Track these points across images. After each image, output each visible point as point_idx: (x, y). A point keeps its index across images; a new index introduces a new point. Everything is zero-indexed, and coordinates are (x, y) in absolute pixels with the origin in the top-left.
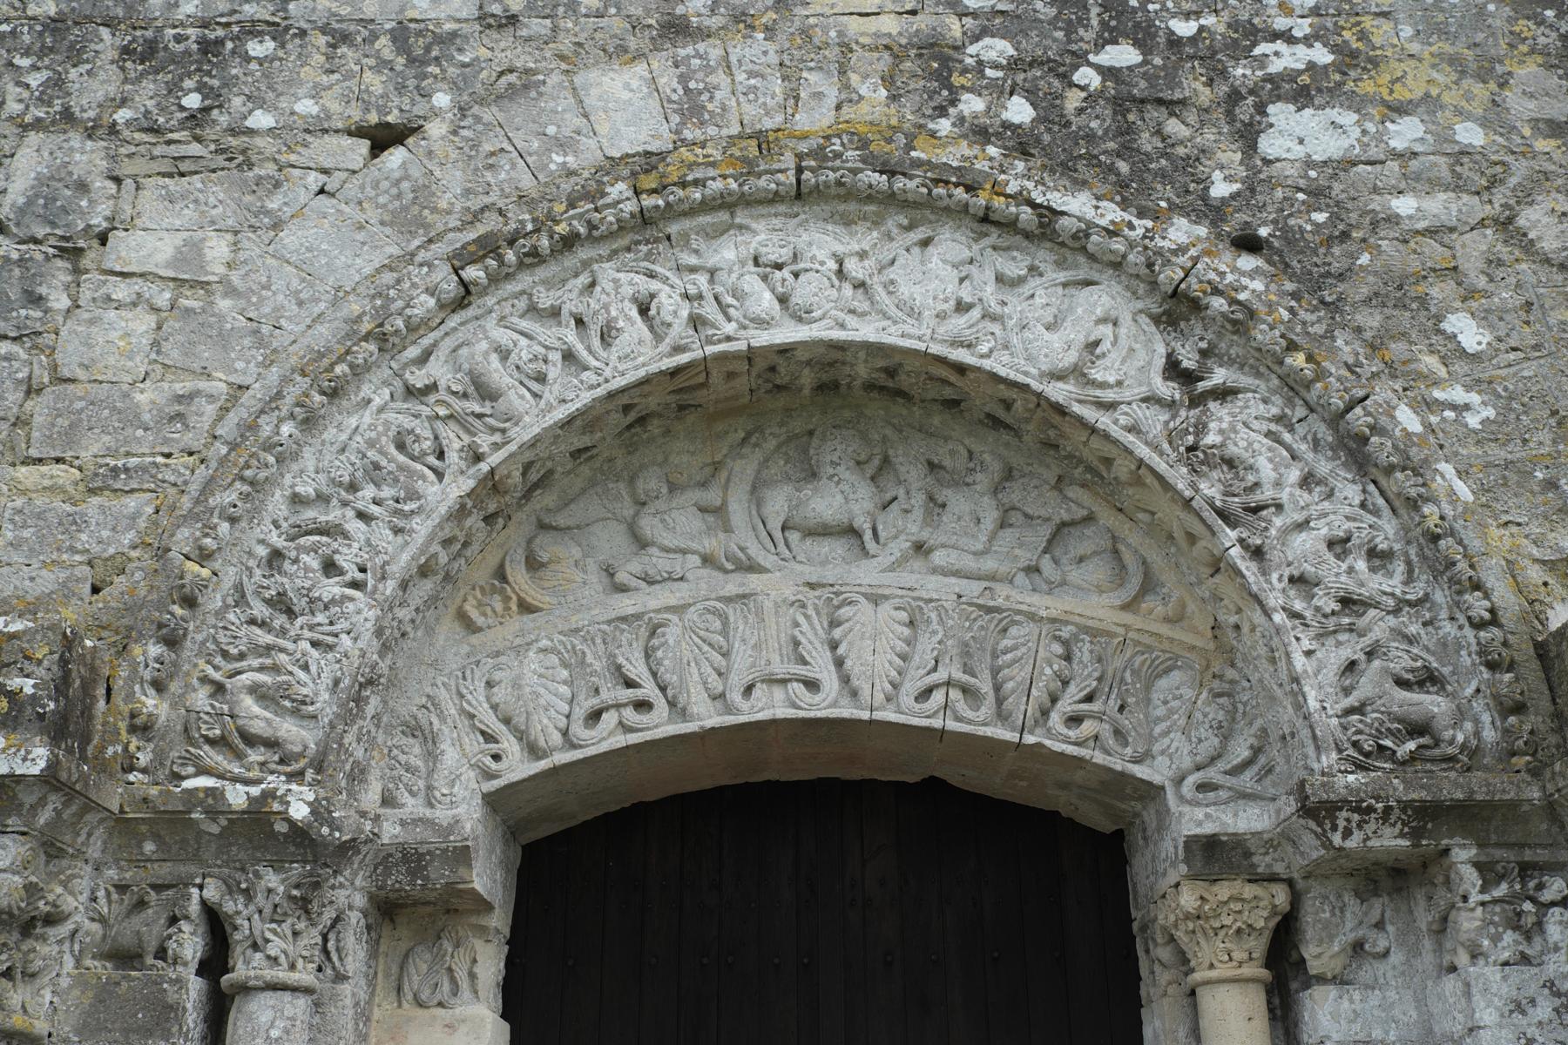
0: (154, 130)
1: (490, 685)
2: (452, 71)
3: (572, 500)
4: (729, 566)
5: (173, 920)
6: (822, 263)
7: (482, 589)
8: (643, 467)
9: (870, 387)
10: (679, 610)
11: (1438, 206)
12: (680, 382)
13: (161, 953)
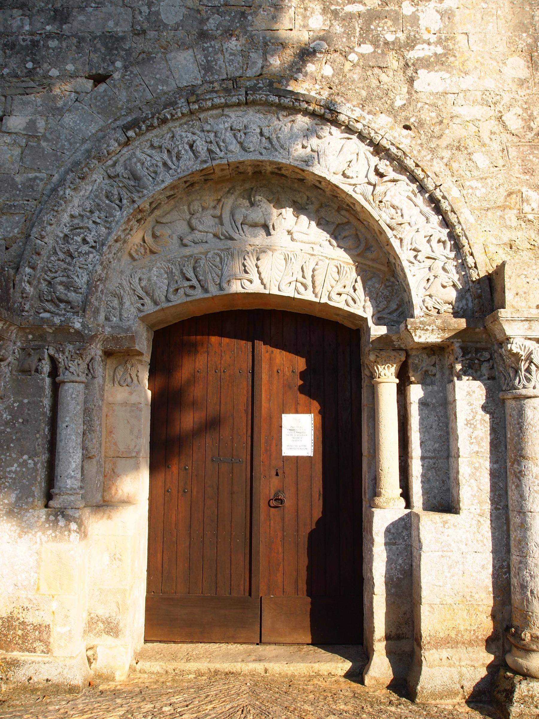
0: (17, 76)
1: (140, 279)
2: (123, 53)
3: (168, 213)
4: (222, 237)
5: (40, 360)
6: (254, 130)
7: (137, 245)
8: (193, 201)
9: (272, 173)
10: (206, 254)
12: (204, 173)
13: (37, 371)
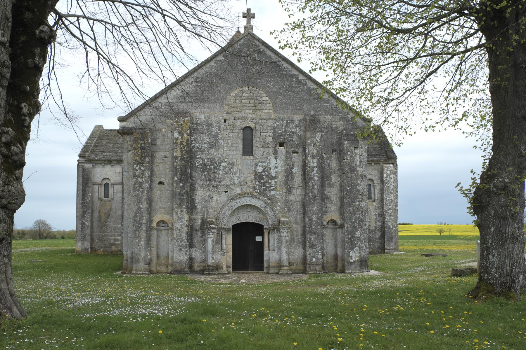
11: (279, 197)
